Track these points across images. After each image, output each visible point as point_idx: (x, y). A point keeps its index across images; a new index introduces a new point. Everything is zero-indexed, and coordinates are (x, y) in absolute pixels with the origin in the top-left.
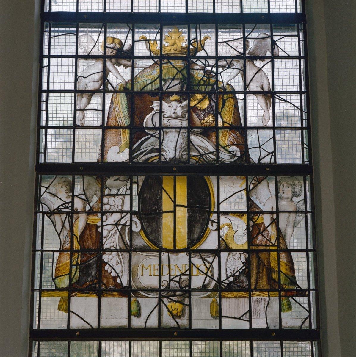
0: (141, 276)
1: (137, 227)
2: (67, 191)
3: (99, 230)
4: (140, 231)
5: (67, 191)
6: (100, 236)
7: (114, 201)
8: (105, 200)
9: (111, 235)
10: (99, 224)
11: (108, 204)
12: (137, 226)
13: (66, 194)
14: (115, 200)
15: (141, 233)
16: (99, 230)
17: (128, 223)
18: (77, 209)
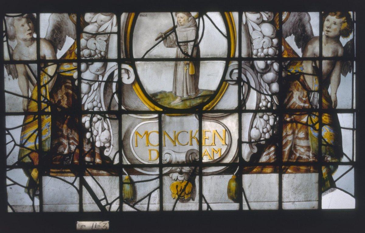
0: (135, 148)
1: (129, 78)
2: (30, 32)
3: (76, 83)
4: (133, 84)
5: (30, 32)
6: (77, 90)
7: (95, 44)
8: (83, 42)
9: (94, 91)
10: (75, 75)
11: (86, 48)
12: (129, 75)
13: (29, 35)
14: (96, 43)
15: (134, 87)
16: (76, 83)
17: (116, 73)
18: (45, 57)
